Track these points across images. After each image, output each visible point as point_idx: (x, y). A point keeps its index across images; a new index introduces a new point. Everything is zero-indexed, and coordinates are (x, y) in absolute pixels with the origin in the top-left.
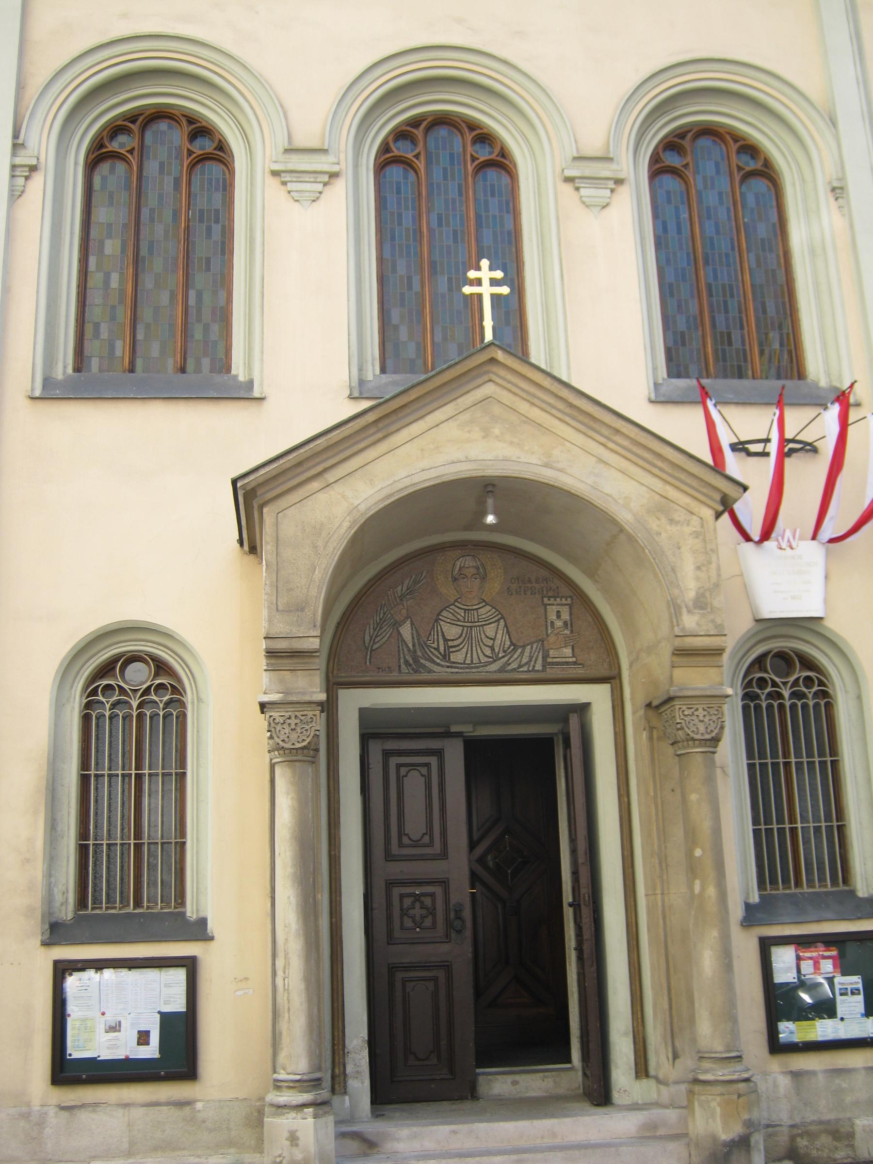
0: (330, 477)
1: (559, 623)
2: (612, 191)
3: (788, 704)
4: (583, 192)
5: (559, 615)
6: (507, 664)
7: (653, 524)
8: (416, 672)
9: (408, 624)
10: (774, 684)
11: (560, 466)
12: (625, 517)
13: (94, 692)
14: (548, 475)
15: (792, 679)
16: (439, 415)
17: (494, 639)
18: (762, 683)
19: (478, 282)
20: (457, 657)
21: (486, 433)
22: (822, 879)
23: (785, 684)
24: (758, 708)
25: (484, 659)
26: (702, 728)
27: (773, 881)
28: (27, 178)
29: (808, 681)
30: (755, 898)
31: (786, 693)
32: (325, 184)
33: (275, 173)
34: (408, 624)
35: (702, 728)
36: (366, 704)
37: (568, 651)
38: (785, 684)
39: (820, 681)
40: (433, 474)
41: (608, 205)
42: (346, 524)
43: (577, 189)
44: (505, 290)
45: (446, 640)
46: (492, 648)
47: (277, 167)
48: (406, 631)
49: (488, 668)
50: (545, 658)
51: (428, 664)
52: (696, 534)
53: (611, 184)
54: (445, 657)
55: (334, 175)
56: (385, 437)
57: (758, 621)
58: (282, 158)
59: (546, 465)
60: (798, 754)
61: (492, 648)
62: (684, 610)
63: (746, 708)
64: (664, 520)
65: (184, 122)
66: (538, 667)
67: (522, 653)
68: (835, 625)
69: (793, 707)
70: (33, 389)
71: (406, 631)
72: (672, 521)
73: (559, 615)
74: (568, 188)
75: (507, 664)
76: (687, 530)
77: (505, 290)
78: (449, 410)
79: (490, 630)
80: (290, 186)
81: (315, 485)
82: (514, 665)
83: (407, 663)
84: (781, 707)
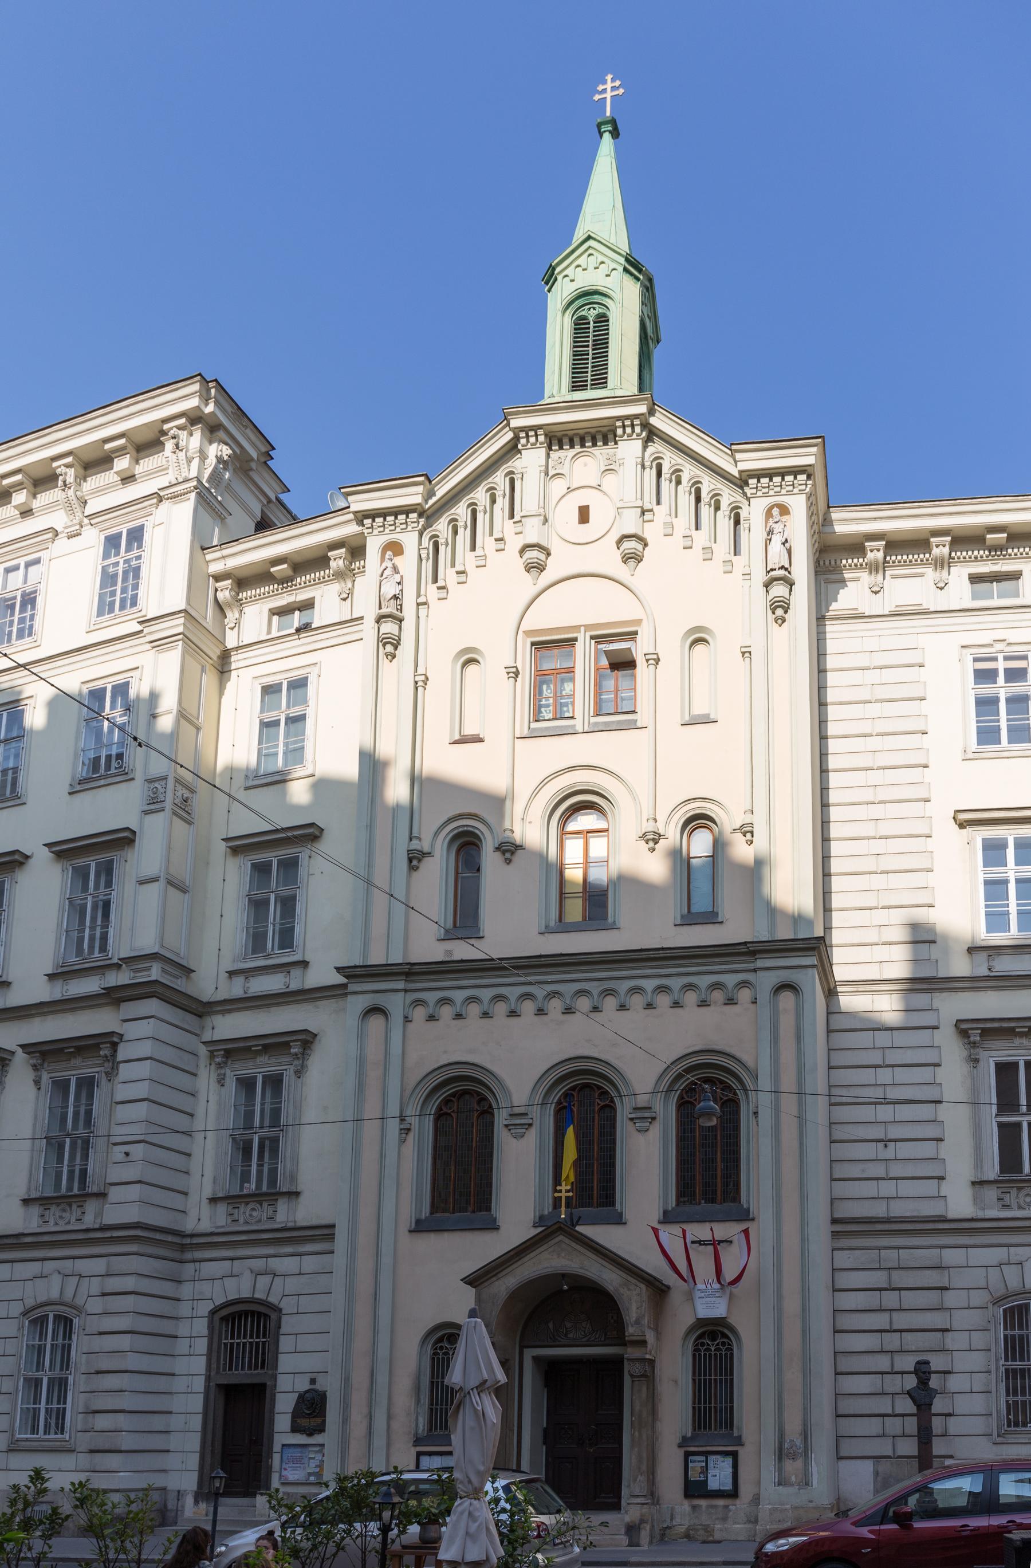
0: (500, 1275)
1: (612, 1321)
2: (650, 1123)
3: (713, 1353)
4: (637, 1125)
5: (612, 1317)
6: (590, 1338)
7: (622, 1290)
8: (554, 1341)
9: (552, 1322)
10: (708, 1345)
11: (586, 1268)
12: (610, 1288)
13: (436, 1349)
14: (581, 1272)
15: (716, 1343)
16: (541, 1249)
17: (585, 1328)
18: (703, 1344)
19: (560, 1191)
20: (571, 1335)
21: (559, 1256)
22: (721, 1427)
23: (713, 1345)
24: (700, 1355)
25: (581, 1336)
26: (637, 1371)
27: (700, 1428)
28: (407, 1134)
29: (723, 1344)
30: (689, 1435)
31: (713, 1349)
32: (527, 1129)
33: (506, 1126)
34: (552, 1322)
35: (637, 1372)
36: (534, 1355)
37: (615, 1333)
38: (713, 1345)
39: (729, 1344)
40: (537, 1273)
41: (648, 1129)
42: (504, 1294)
43: (635, 1123)
44: (571, 1194)
45: (566, 1329)
46: (584, 1332)
47: (506, 1122)
48: (551, 1325)
49: (583, 1340)
50: (605, 1336)
51: (559, 1338)
52: (638, 1295)
53: (650, 1120)
54: (566, 1335)
55: (530, 1125)
56: (520, 1259)
57: (698, 1319)
58: (509, 1118)
59: (581, 1268)
60: (716, 1375)
61: (584, 1332)
62: (630, 1325)
63: (694, 1355)
64: (626, 1289)
65: (475, 1095)
66: (603, 1339)
67: (596, 1334)
68: (732, 1321)
69: (715, 1355)
70: (411, 1226)
71: (551, 1325)
72: (629, 1289)
73: (612, 1317)
74: (631, 1123)
75: (590, 1338)
76: (634, 1293)
77: (571, 1194)
78: (545, 1247)
79: (584, 1324)
80: (512, 1131)
81: (494, 1279)
82: (593, 1339)
83: (550, 1338)
84: (710, 1355)
